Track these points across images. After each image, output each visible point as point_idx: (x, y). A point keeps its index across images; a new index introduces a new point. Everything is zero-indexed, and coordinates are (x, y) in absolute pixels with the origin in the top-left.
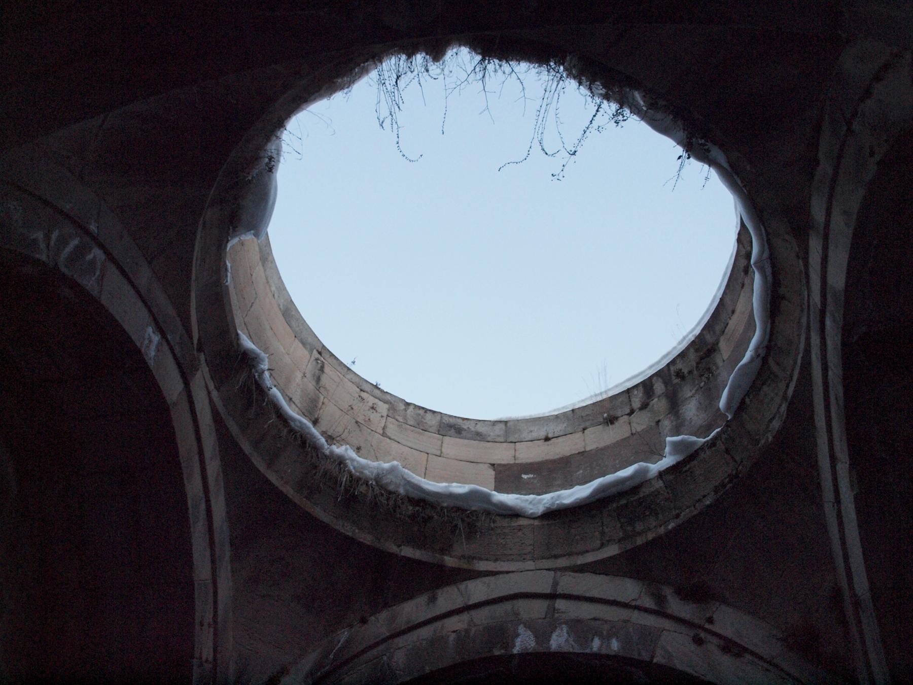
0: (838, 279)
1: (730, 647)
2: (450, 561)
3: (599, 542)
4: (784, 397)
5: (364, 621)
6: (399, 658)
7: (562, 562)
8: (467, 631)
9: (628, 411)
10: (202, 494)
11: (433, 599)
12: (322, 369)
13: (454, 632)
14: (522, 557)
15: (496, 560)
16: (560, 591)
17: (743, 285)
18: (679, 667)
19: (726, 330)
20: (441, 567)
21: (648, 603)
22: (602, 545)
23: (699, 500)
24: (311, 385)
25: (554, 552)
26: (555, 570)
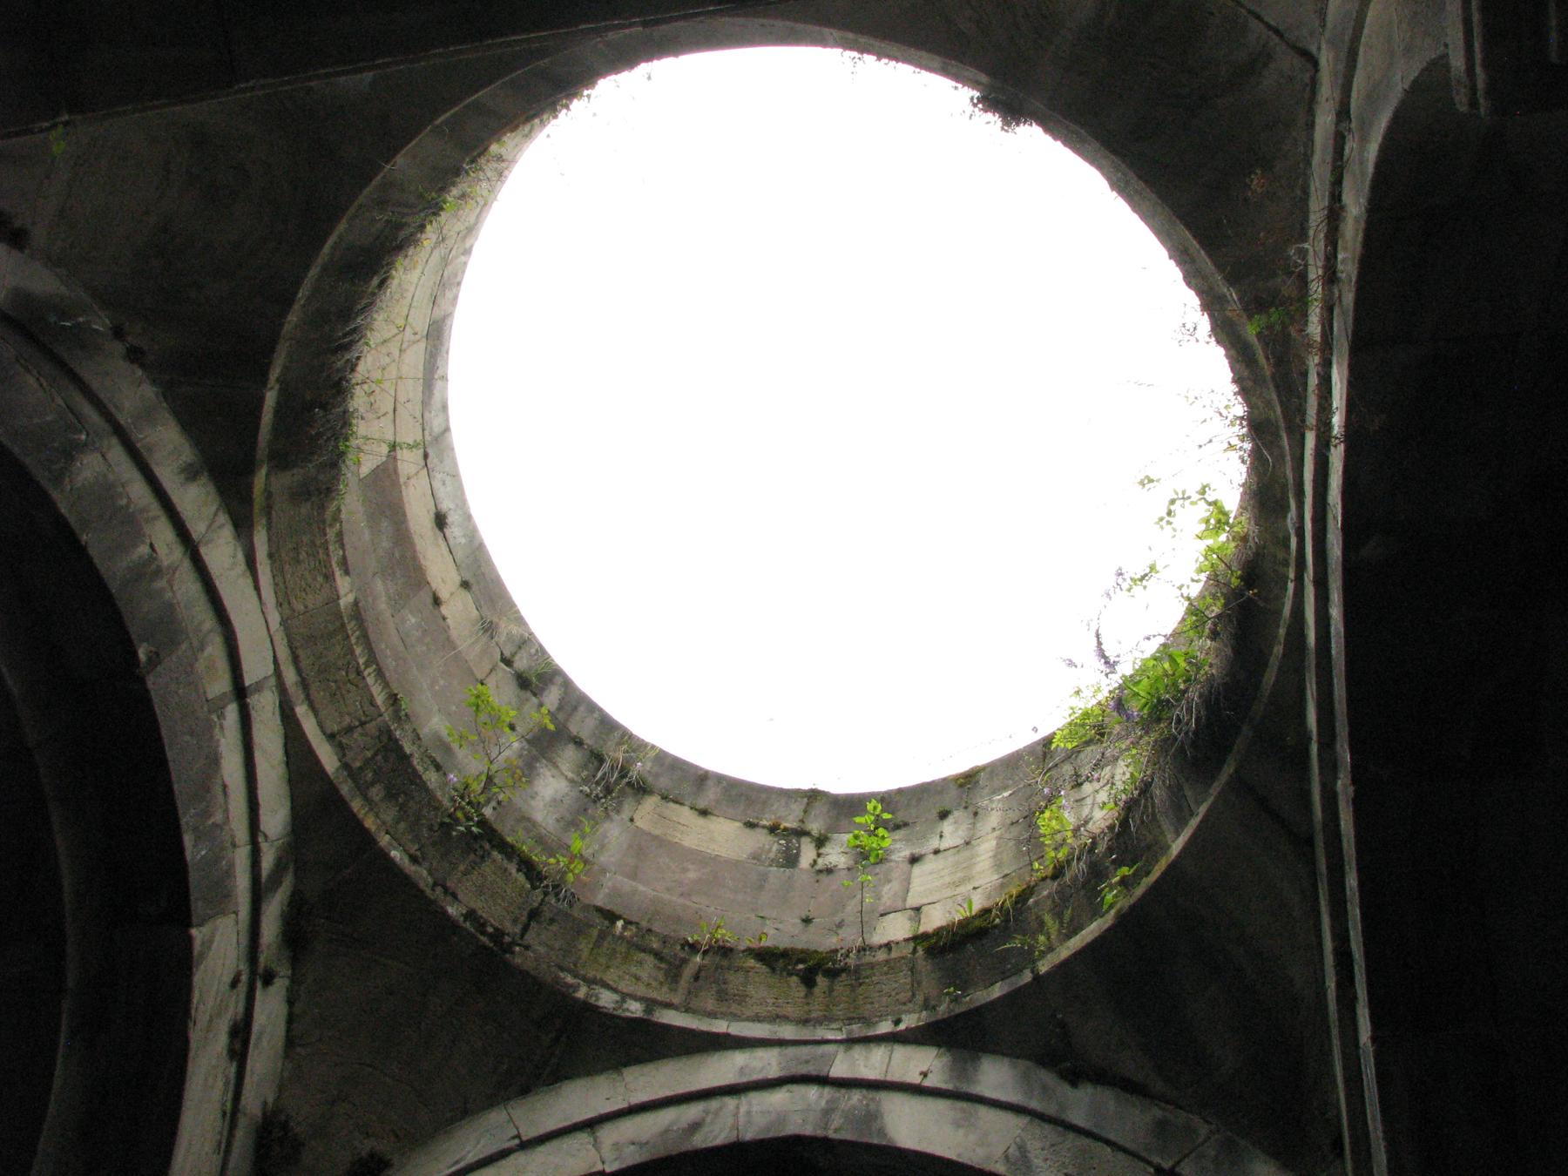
1: (241, 1033)
3: (336, 728)
4: (651, 1004)
5: (135, 355)
6: (88, 468)
7: (290, 676)
8: (158, 572)
9: (507, 654)
11: (191, 473)
13: (152, 546)
15: (271, 556)
17: (751, 825)
19: (671, 805)
20: (249, 468)
21: (267, 862)
22: (331, 737)
23: (446, 890)
26: (278, 672)
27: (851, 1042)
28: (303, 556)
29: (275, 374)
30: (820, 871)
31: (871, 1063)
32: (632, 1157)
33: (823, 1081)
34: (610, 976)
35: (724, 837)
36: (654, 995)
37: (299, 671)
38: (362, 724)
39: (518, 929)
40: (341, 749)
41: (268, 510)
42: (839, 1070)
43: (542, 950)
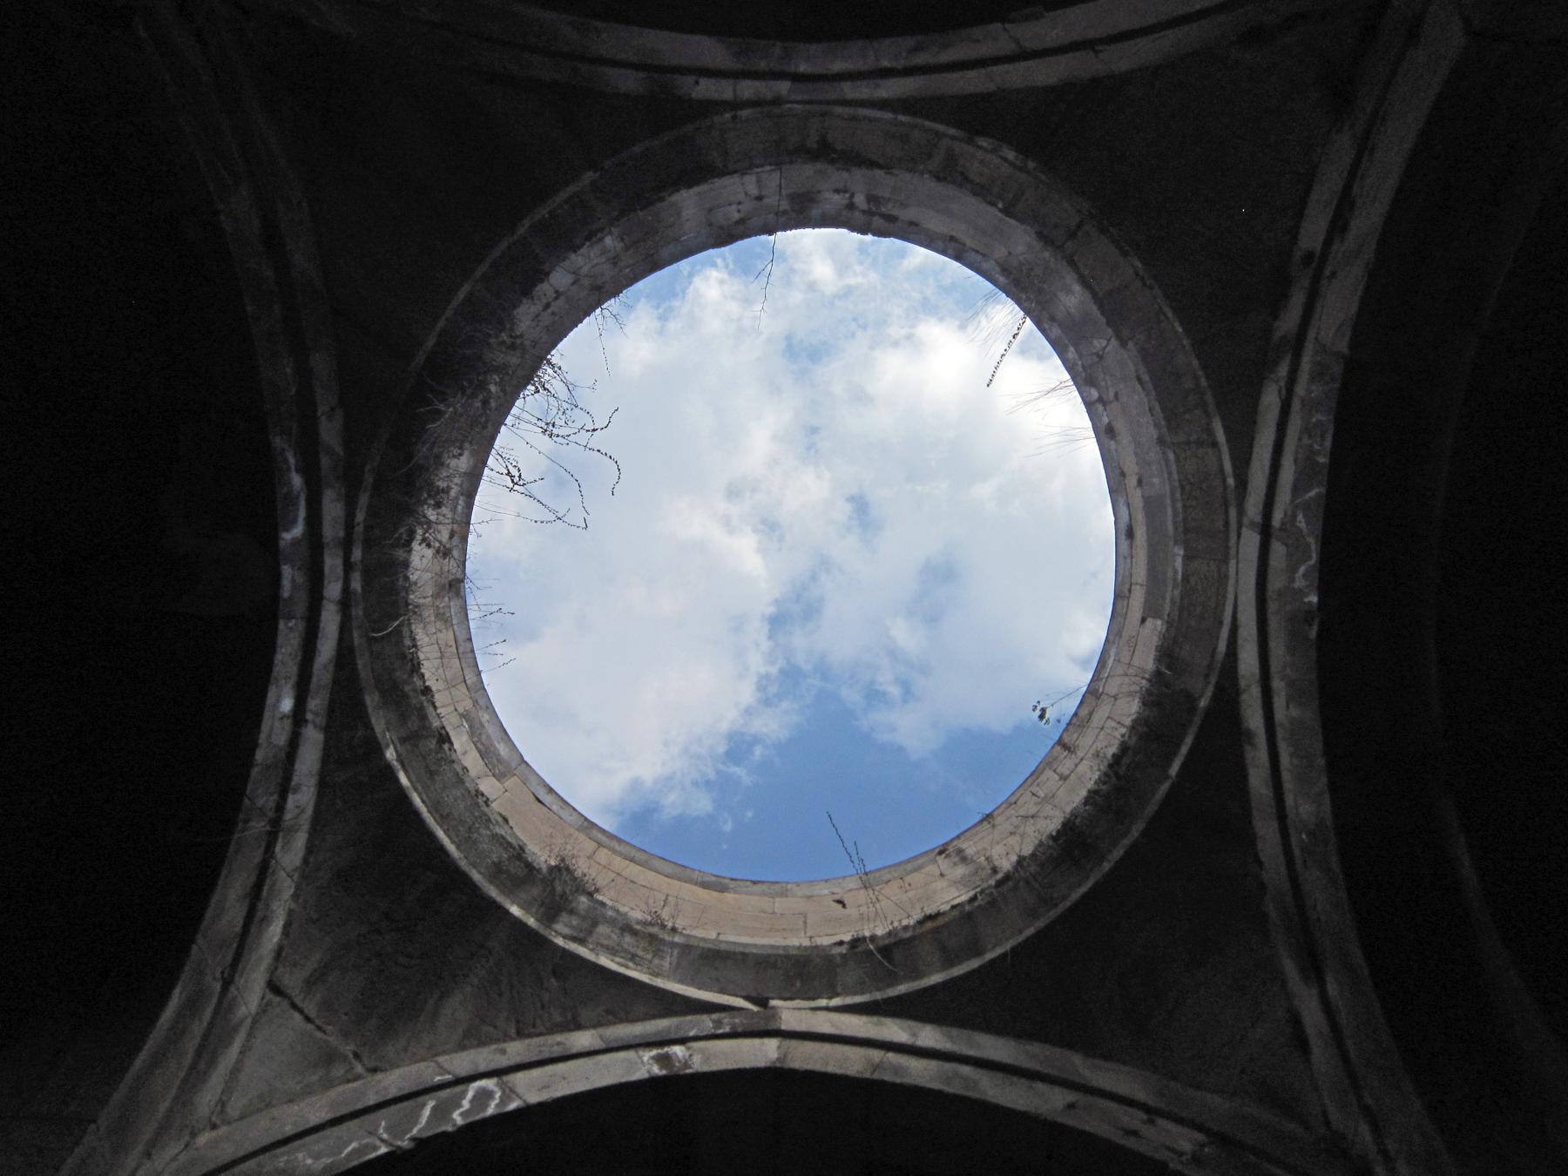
0: (708, 50)
2: (1203, 703)
3: (1210, 451)
4: (970, 142)
7: (1233, 512)
8: (1291, 684)
10: (948, 1066)
12: (960, 851)
14: (1223, 579)
15: (1221, 623)
16: (1258, 519)
18: (1354, 309)
20: (1208, 712)
21: (1283, 370)
22: (1215, 444)
23: (1143, 279)
24: (961, 870)
25: (1220, 524)
26: (1240, 526)
27: (777, 101)
28: (1199, 610)
29: (1164, 788)
30: (845, 191)
31: (748, 89)
32: (977, 32)
33: (797, 78)
34: (1005, 169)
35: (935, 223)
36: (966, 147)
37: (1227, 512)
38: (1188, 443)
39: (1086, 228)
40: (1209, 431)
41: (1210, 667)
42: (783, 87)
43: (1066, 205)
